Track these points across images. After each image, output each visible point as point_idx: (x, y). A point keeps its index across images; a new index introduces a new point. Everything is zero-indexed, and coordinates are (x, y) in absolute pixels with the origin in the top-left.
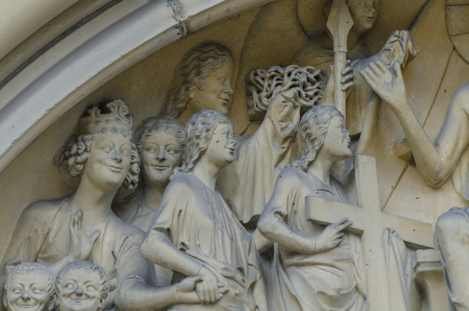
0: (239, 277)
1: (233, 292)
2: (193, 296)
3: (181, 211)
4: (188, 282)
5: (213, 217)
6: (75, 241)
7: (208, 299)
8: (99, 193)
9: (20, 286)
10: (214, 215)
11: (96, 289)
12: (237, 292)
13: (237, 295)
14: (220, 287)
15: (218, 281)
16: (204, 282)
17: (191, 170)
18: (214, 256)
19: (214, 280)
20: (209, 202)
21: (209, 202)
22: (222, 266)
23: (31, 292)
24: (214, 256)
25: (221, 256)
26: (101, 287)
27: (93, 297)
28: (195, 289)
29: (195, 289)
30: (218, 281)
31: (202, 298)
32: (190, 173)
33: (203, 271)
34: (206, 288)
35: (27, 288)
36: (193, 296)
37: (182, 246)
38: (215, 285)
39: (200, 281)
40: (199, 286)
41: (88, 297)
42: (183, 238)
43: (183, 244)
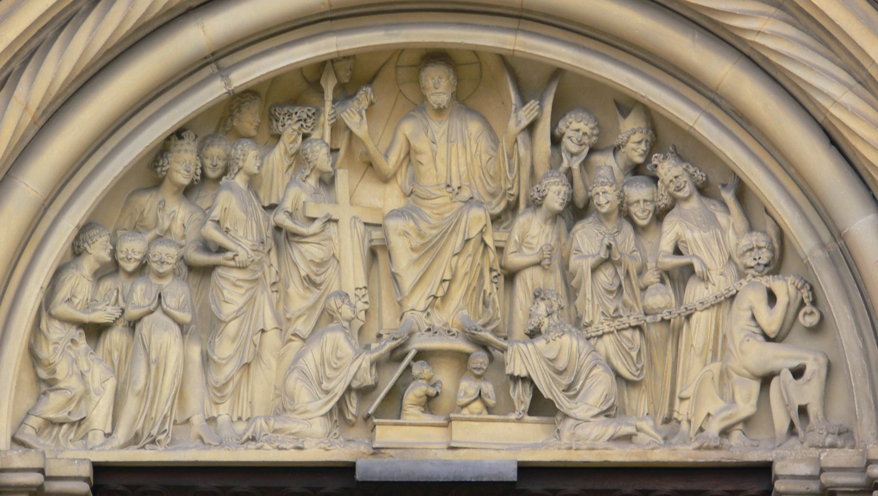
0: (261, 248)
1: (257, 259)
2: (232, 263)
3: (226, 208)
4: (229, 255)
5: (246, 212)
6: (160, 221)
7: (241, 265)
8: (176, 189)
9: (125, 250)
10: (247, 211)
11: (172, 258)
12: (259, 258)
13: (259, 260)
14: (248, 258)
15: (248, 254)
16: (240, 256)
17: (233, 179)
18: (246, 238)
19: (245, 253)
20: (244, 201)
21: (244, 201)
22: (250, 243)
23: (133, 254)
24: (246, 238)
25: (250, 237)
26: (176, 257)
27: (171, 264)
28: (233, 259)
29: (233, 259)
30: (248, 254)
31: (238, 265)
32: (232, 181)
33: (239, 249)
34: (241, 260)
35: (130, 252)
36: (232, 263)
37: (226, 230)
38: (246, 258)
39: (237, 255)
40: (236, 258)
41: (168, 263)
42: (228, 225)
43: (227, 228)
